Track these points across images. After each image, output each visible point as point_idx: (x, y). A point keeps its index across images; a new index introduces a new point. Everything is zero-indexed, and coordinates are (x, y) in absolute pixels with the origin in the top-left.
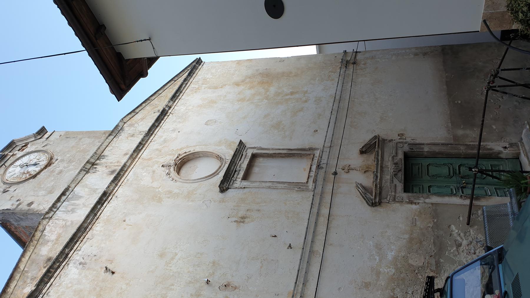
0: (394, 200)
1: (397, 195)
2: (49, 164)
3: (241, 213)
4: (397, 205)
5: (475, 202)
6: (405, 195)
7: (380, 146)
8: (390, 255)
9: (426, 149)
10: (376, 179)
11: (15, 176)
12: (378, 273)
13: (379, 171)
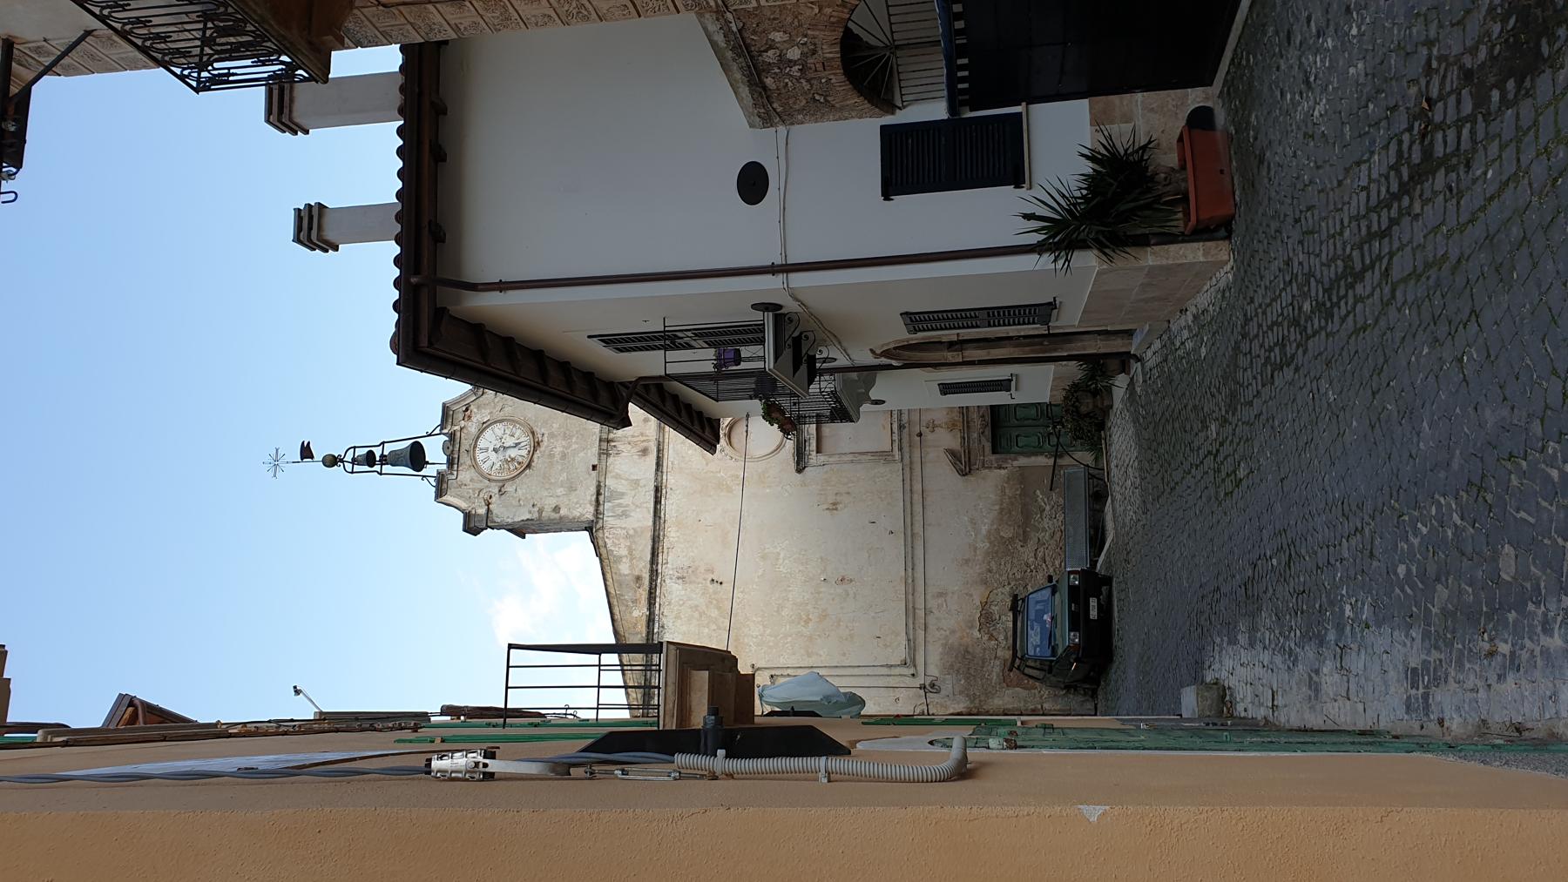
2: (537, 445)
3: (831, 499)
5: (1059, 461)
6: (993, 457)
8: (984, 529)
11: (497, 466)
12: (975, 549)
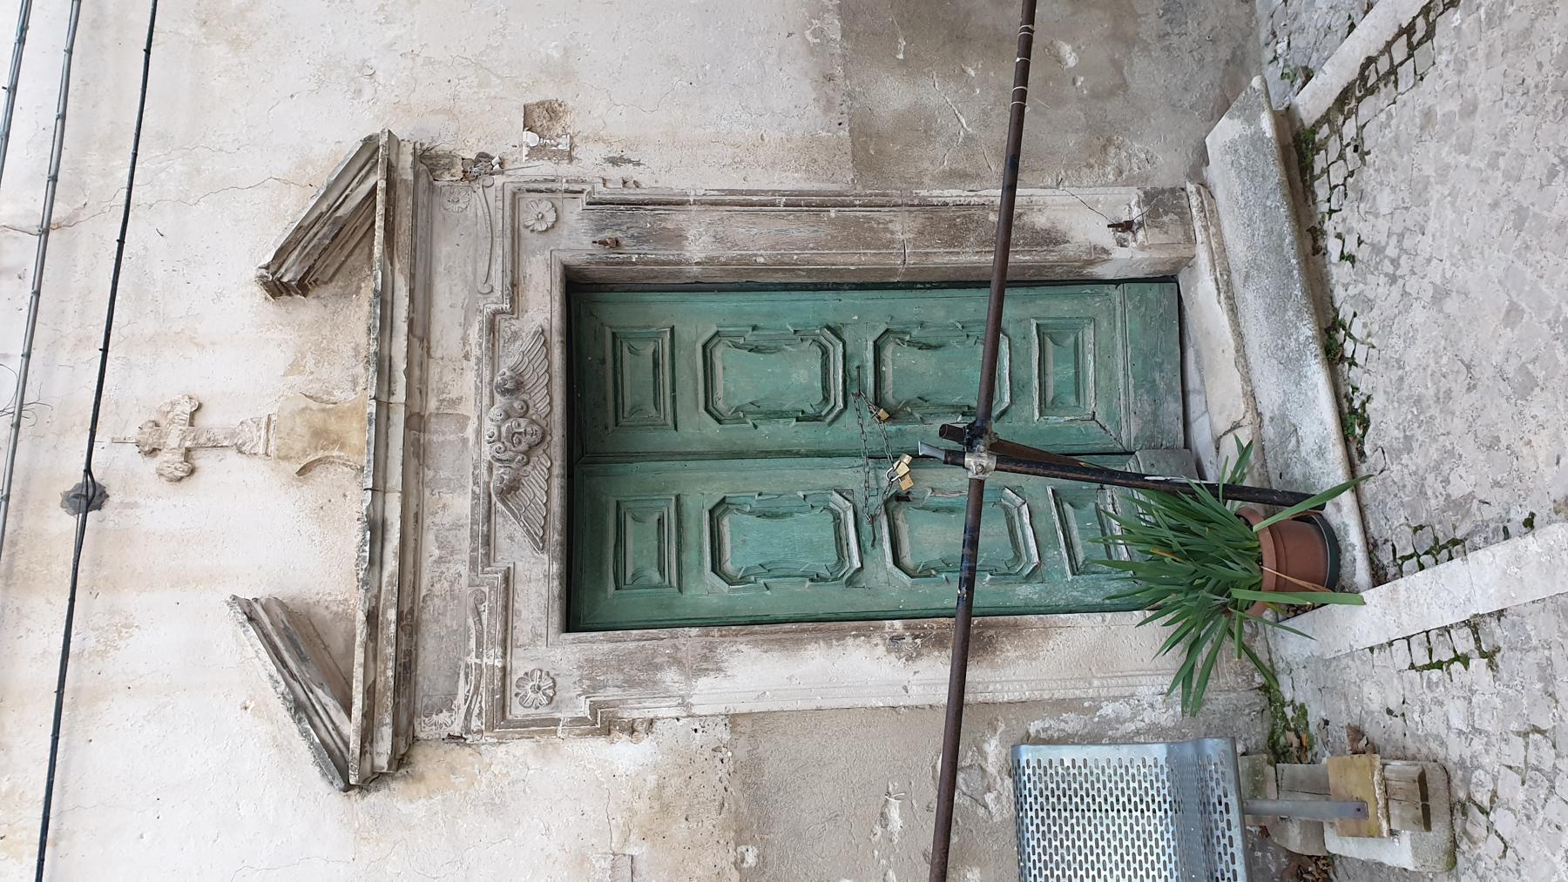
0: (499, 717)
1: (520, 665)
4: (520, 748)
6: (568, 655)
7: (403, 237)
9: (698, 245)
10: (375, 561)
13: (395, 479)
